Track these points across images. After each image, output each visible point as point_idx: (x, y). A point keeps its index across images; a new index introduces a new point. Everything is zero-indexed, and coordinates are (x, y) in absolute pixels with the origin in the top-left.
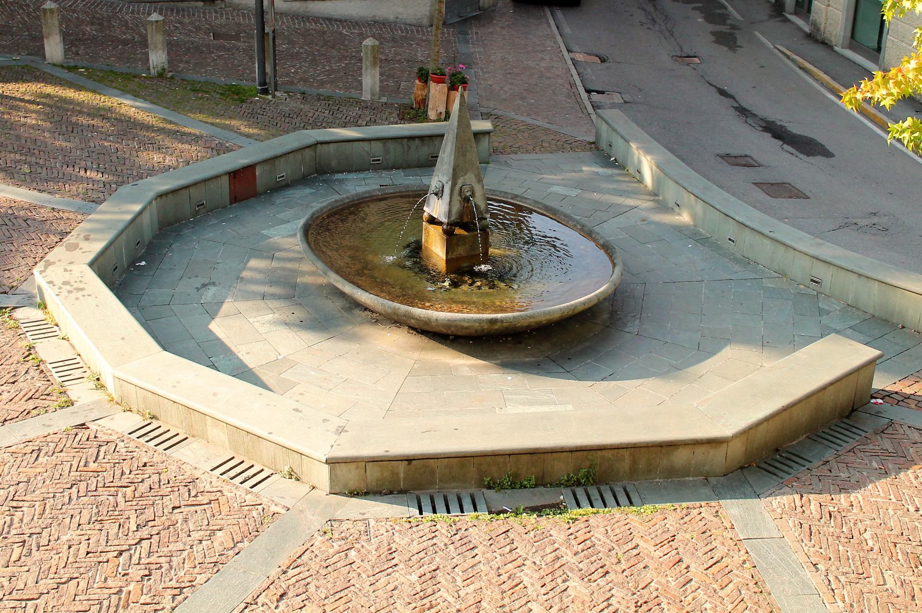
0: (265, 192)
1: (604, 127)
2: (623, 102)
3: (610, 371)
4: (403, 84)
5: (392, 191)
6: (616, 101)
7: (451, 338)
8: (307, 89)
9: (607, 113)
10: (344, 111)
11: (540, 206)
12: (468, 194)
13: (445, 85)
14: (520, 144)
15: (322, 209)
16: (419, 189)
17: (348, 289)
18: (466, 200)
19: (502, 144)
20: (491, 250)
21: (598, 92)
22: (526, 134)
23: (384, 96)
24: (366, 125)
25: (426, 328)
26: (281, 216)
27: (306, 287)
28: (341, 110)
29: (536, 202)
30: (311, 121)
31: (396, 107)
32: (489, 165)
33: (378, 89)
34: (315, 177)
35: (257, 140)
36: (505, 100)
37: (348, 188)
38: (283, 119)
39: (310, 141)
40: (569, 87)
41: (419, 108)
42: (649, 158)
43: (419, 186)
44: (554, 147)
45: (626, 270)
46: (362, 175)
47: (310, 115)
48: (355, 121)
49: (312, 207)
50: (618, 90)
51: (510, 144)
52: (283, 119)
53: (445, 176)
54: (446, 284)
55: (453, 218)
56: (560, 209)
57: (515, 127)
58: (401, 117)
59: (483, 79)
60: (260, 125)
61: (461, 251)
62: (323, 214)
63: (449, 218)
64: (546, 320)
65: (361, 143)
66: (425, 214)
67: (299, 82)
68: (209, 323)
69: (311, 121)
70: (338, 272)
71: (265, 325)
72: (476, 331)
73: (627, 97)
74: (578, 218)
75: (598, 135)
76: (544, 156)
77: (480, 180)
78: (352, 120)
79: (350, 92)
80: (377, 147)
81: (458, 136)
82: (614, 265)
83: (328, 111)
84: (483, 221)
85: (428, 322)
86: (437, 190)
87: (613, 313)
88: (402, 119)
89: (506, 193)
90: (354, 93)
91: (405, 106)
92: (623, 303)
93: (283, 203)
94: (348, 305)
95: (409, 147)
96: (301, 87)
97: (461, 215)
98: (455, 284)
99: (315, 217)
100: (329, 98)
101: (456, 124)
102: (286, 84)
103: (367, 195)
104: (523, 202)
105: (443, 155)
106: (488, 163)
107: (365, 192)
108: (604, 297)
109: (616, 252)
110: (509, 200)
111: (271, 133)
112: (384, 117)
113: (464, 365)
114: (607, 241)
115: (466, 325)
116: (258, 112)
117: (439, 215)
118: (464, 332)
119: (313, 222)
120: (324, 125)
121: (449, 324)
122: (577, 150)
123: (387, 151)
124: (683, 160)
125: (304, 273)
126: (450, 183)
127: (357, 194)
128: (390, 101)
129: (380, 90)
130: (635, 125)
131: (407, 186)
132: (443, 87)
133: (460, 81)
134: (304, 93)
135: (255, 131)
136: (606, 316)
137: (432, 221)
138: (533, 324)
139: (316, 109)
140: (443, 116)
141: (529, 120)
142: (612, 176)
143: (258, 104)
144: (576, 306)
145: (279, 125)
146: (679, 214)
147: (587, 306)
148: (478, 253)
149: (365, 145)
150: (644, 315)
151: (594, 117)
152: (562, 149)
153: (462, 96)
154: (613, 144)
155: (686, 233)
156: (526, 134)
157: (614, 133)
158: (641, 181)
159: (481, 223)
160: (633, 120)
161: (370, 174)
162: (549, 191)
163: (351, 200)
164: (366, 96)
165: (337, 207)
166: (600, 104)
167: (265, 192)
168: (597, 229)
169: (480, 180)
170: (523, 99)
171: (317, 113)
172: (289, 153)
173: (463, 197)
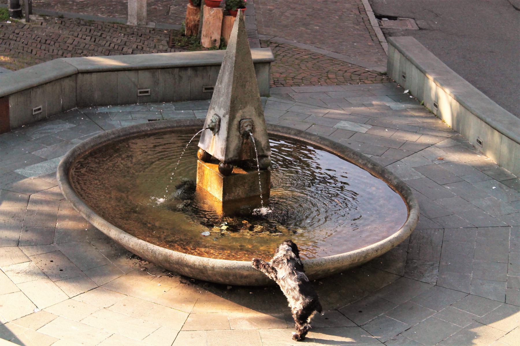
0: (20, 127)
1: (397, 56)
2: (418, 29)
3: (406, 325)
4: (173, 8)
5: (161, 126)
6: (409, 27)
7: (229, 288)
8: (66, 12)
9: (402, 41)
10: (108, 38)
11: (326, 143)
12: (248, 129)
13: (220, 9)
14: (303, 75)
15: (84, 145)
16: (192, 123)
17: (114, 233)
18: (246, 135)
19: (283, 75)
20: (272, 193)
21: (390, 18)
22: (310, 65)
23: (152, 21)
24: (132, 53)
25: (200, 277)
26: (39, 153)
27: (66, 233)
28: (103, 36)
29: (322, 139)
30: (70, 49)
31: (166, 34)
32: (270, 98)
33: (145, 14)
34: (77, 110)
35: (9, 69)
36: (286, 26)
37: (113, 123)
38: (39, 46)
39: (69, 70)
40: (358, 13)
41: (191, 35)
42: (448, 90)
43: (192, 120)
44: (341, 79)
45: (423, 213)
46: (128, 109)
47: (70, 41)
48: (120, 48)
49: (72, 144)
50: (412, 15)
51: (292, 75)
52: (39, 46)
53: (222, 109)
54: (224, 227)
55: (231, 155)
56: (348, 146)
57: (298, 56)
58: (171, 44)
59: (261, 3)
60: (12, 52)
61: (239, 192)
62: (85, 151)
63: (226, 155)
64: (334, 268)
65: (127, 73)
66: (200, 151)
67: (56, 5)
69: (70, 49)
70: (104, 215)
71: (20, 275)
72: (257, 280)
73: (422, 23)
74: (369, 156)
75: (390, 65)
76: (330, 89)
77: (260, 114)
78: (116, 47)
79: (114, 17)
80: (145, 78)
81: (237, 66)
82: (410, 208)
83: (90, 37)
84: (264, 159)
85: (203, 270)
86: (213, 124)
87: (408, 262)
88: (173, 46)
89: (289, 128)
90: (118, 18)
91: (175, 33)
92: (420, 250)
93: (39, 139)
94: (113, 252)
95: (181, 77)
96: (59, 10)
97: (240, 151)
98: (233, 228)
99: (76, 154)
100: (90, 23)
101: (234, 51)
102: (42, 6)
103: (135, 130)
104: (308, 139)
105: (220, 86)
106: (268, 96)
107: (132, 127)
108: (398, 243)
109: (411, 193)
110: (292, 137)
111: (26, 61)
112: (152, 45)
113: (243, 319)
114: (402, 182)
115: (245, 273)
116: (11, 37)
117: (216, 152)
118: (243, 282)
119: (75, 159)
120: (85, 52)
121: (227, 272)
122: (366, 81)
123: (156, 83)
124: (485, 92)
125: (63, 218)
126: (227, 116)
127: (124, 129)
128: (159, 27)
129: (148, 15)
130: (431, 55)
131: (179, 121)
132: (218, 12)
133: (237, 5)
134: (61, 17)
135: (7, 59)
136: (400, 264)
137: (208, 158)
138: (320, 272)
139: (76, 34)
140: (218, 44)
141: (313, 49)
142: (405, 110)
143: (10, 28)
144: (367, 253)
145: (34, 52)
146: (483, 153)
147: (379, 253)
148: (258, 193)
149: (132, 75)
150: (444, 264)
151: (385, 45)
152: (351, 80)
153: (241, 20)
154: (407, 75)
155: (490, 173)
156: (310, 65)
157: (408, 63)
158: (438, 116)
159: (262, 161)
160: (429, 49)
161: (138, 108)
162: (335, 126)
163: (116, 135)
164: (132, 21)
165: (101, 143)
166: (391, 31)
167: (20, 127)
168: (390, 168)
169: (260, 114)
170: (306, 25)
171: (77, 40)
172: (46, 83)
173: (242, 132)
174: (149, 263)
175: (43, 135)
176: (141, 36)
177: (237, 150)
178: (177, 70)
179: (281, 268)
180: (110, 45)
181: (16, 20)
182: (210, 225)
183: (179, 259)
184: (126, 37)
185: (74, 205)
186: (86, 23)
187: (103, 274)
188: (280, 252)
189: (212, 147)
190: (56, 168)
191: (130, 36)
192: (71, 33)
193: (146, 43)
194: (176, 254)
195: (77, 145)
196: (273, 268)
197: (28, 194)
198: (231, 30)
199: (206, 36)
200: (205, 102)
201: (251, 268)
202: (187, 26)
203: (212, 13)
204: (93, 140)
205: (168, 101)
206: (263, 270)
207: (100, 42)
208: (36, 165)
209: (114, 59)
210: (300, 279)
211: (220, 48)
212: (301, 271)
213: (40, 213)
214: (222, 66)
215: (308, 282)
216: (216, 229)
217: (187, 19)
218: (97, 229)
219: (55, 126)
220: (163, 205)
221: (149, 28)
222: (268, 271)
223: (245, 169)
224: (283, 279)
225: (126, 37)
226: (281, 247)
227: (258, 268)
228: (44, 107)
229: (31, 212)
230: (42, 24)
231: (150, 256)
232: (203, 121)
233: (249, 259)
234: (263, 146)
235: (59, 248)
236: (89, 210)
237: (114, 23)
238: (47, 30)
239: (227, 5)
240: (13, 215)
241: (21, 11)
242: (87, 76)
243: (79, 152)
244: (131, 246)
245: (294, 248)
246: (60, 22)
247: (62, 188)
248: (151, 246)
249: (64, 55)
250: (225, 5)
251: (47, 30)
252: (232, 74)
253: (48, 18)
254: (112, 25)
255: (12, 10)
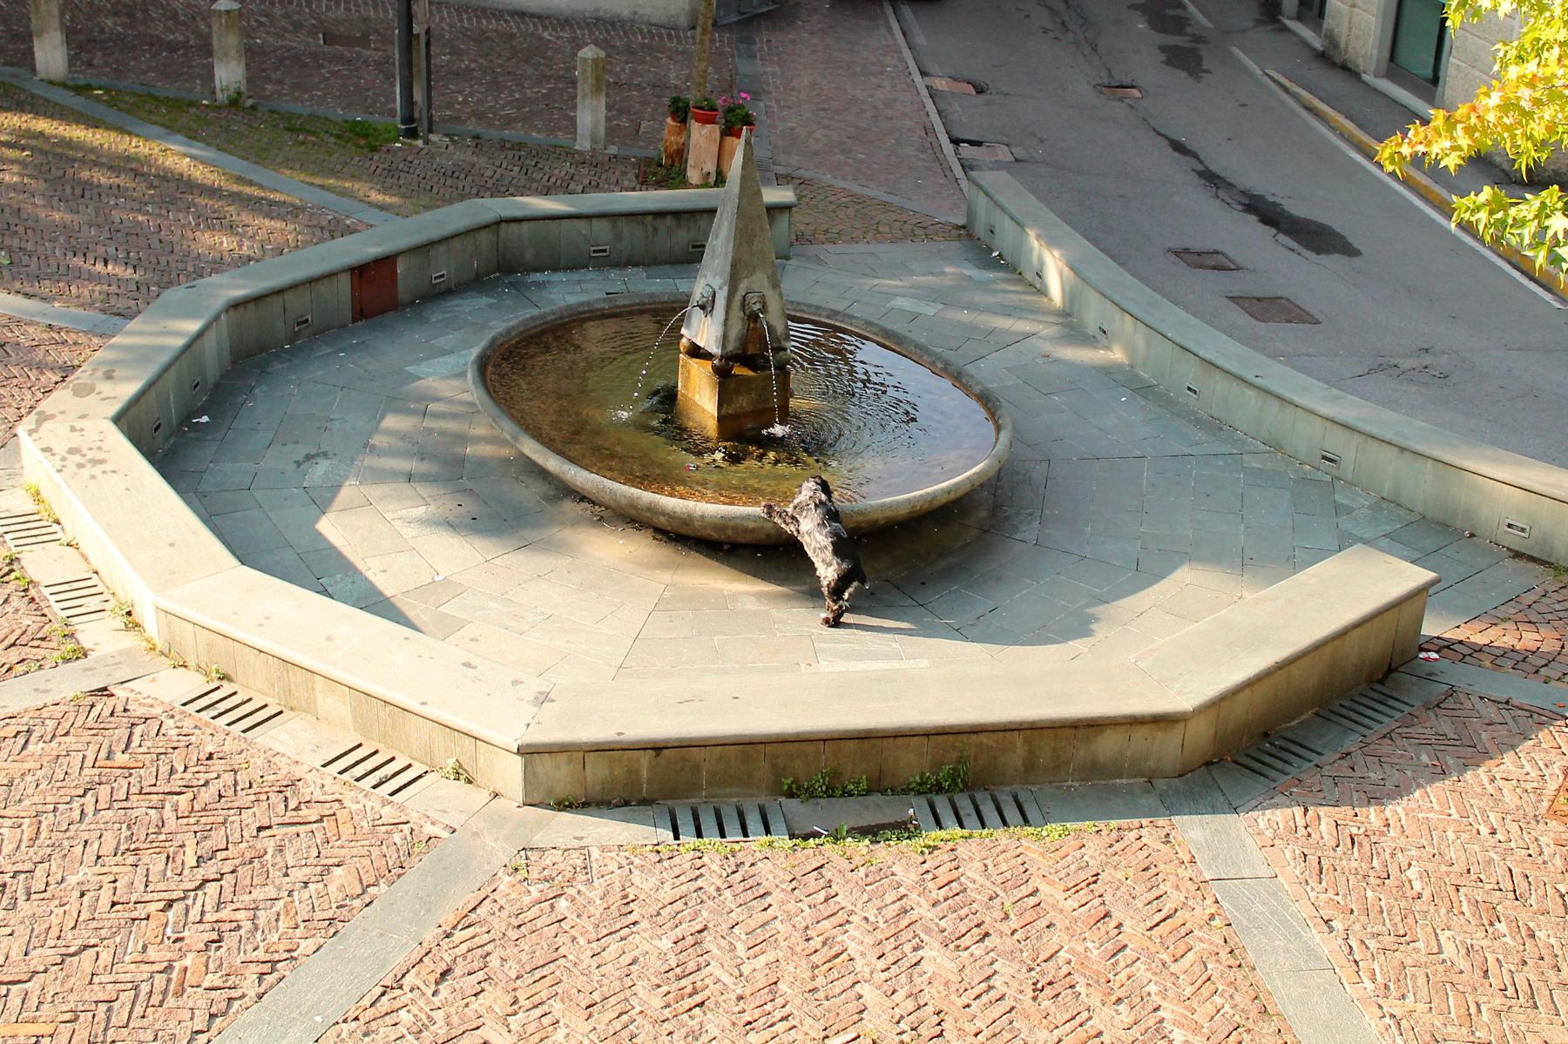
0: (412, 303)
1: (981, 201)
2: (1012, 159)
3: (991, 604)
4: (645, 124)
5: (626, 302)
6: (1001, 157)
7: (726, 547)
8: (483, 130)
9: (987, 178)
10: (547, 169)
11: (874, 329)
12: (756, 308)
13: (717, 126)
14: (840, 227)
15: (509, 331)
16: (673, 298)
17: (553, 463)
18: (753, 317)
19: (812, 227)
20: (792, 403)
21: (972, 143)
22: (851, 212)
23: (613, 144)
24: (582, 192)
25: (684, 530)
26: (440, 342)
27: (481, 463)
28: (540, 166)
29: (869, 323)
30: (489, 185)
31: (633, 164)
32: (790, 262)
33: (602, 132)
34: (498, 278)
35: (397, 215)
36: (816, 153)
37: (552, 296)
38: (442, 181)
39: (489, 217)
40: (923, 134)
41: (672, 166)
42: (1056, 253)
43: (672, 293)
44: (899, 233)
45: (1018, 437)
46: (576, 276)
47: (489, 173)
48: (565, 184)
49: (491, 328)
50: (1005, 140)
51: (824, 227)
52: (442, 181)
53: (718, 277)
54: (718, 456)
55: (730, 347)
56: (908, 334)
57: (833, 198)
58: (641, 179)
59: (779, 119)
60: (403, 190)
61: (743, 403)
62: (511, 340)
63: (724, 347)
64: (885, 518)
65: (575, 221)
66: (684, 340)
67: (469, 118)
68: (317, 520)
69: (489, 185)
70: (538, 436)
71: (412, 525)
72: (768, 536)
73: (1020, 152)
74: (940, 350)
75: (971, 214)
76: (883, 247)
77: (775, 285)
78: (559, 183)
79: (556, 136)
80: (601, 229)
81: (741, 212)
82: (998, 429)
83: (518, 168)
84: (781, 353)
85: (687, 520)
86: (705, 299)
87: (995, 509)
88: (644, 182)
89: (818, 308)
90: (561, 138)
91: (648, 162)
92: (1012, 492)
93: (442, 321)
94: (551, 493)
95: (655, 230)
96: (472, 126)
97: (744, 341)
98: (733, 459)
99: (498, 343)
100: (520, 146)
101: (737, 190)
102: (448, 120)
103: (586, 309)
104: (847, 323)
105: (715, 242)
106: (788, 258)
107: (582, 304)
108: (981, 481)
109: (1000, 406)
110: (823, 320)
111: (423, 203)
112: (613, 180)
113: (747, 593)
114: (988, 390)
115: (751, 525)
116: (401, 167)
117: (708, 341)
118: (747, 539)
119: (495, 352)
120: (512, 190)
121: (723, 524)
122: (935, 238)
123: (618, 237)
124: (1111, 257)
125: (477, 440)
126: (726, 289)
127: (569, 307)
128: (623, 153)
129: (606, 134)
130: (1033, 198)
131: (653, 295)
132: (713, 131)
133: (742, 120)
134: (476, 137)
135: (395, 200)
136: (983, 514)
137: (696, 352)
138: (863, 525)
139: (498, 164)
140: (712, 180)
141: (856, 188)
142: (993, 281)
143: (400, 154)
144: (934, 495)
145: (435, 190)
146: (1107, 348)
147: (953, 496)
148: (771, 405)
149: (582, 225)
150: (1047, 512)
151: (964, 184)
152: (912, 236)
153: (748, 143)
154: (997, 231)
155: (1118, 377)
156: (851, 212)
157: (999, 211)
158: (1042, 291)
159: (778, 357)
160: (1029, 190)
161: (590, 274)
162: (889, 305)
163: (558, 315)
164: (583, 144)
165: (534, 327)
166: (974, 163)
167: (412, 303)
168: (970, 369)
169: (775, 285)
170: (845, 151)
171: (499, 170)
172: (453, 237)
173: (747, 312)
174: (607, 509)
175: (447, 315)
176: (596, 166)
177: (740, 339)
178: (650, 218)
179: (805, 517)
180: (548, 180)
181: (409, 141)
182: (699, 454)
183: (651, 503)
184: (574, 166)
185: (494, 420)
186: (513, 145)
187: (536, 525)
188: (804, 492)
189: (702, 335)
190: (466, 364)
191: (580, 166)
192: (492, 161)
193: (604, 177)
194: (646, 496)
195: (499, 330)
196: (793, 518)
197: (425, 403)
198: (732, 159)
199: (694, 167)
200: (692, 266)
201: (760, 517)
202: (666, 151)
203: (703, 132)
204: (521, 323)
205: (636, 265)
206: (778, 520)
207: (534, 175)
208: (436, 360)
209: (557, 201)
210: (835, 534)
211: (716, 185)
212: (836, 522)
213: (443, 433)
214: (718, 214)
215: (845, 539)
216: (707, 458)
217: (667, 140)
218: (528, 458)
219: (465, 302)
220: (626, 424)
221: (608, 154)
222: (785, 522)
223: (753, 369)
224: (809, 534)
225: (574, 166)
226: (805, 485)
227: (771, 517)
228: (449, 273)
229: (431, 431)
230: (447, 148)
231: (606, 499)
232: (689, 296)
233: (757, 504)
234: (779, 333)
235: (470, 485)
236: (516, 429)
237: (555, 146)
238: (455, 157)
239: (727, 121)
240: (403, 436)
241: (416, 128)
242: (514, 226)
243: (501, 341)
244: (578, 483)
245: (825, 487)
246: (474, 144)
247: (475, 395)
248: (609, 483)
249: (481, 195)
250: (724, 121)
251: (455, 157)
252: (734, 224)
253: (456, 138)
254: (552, 149)
255: (403, 127)
